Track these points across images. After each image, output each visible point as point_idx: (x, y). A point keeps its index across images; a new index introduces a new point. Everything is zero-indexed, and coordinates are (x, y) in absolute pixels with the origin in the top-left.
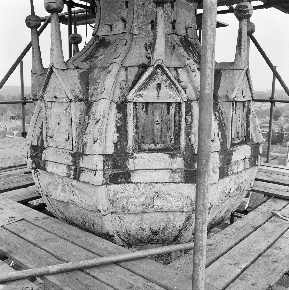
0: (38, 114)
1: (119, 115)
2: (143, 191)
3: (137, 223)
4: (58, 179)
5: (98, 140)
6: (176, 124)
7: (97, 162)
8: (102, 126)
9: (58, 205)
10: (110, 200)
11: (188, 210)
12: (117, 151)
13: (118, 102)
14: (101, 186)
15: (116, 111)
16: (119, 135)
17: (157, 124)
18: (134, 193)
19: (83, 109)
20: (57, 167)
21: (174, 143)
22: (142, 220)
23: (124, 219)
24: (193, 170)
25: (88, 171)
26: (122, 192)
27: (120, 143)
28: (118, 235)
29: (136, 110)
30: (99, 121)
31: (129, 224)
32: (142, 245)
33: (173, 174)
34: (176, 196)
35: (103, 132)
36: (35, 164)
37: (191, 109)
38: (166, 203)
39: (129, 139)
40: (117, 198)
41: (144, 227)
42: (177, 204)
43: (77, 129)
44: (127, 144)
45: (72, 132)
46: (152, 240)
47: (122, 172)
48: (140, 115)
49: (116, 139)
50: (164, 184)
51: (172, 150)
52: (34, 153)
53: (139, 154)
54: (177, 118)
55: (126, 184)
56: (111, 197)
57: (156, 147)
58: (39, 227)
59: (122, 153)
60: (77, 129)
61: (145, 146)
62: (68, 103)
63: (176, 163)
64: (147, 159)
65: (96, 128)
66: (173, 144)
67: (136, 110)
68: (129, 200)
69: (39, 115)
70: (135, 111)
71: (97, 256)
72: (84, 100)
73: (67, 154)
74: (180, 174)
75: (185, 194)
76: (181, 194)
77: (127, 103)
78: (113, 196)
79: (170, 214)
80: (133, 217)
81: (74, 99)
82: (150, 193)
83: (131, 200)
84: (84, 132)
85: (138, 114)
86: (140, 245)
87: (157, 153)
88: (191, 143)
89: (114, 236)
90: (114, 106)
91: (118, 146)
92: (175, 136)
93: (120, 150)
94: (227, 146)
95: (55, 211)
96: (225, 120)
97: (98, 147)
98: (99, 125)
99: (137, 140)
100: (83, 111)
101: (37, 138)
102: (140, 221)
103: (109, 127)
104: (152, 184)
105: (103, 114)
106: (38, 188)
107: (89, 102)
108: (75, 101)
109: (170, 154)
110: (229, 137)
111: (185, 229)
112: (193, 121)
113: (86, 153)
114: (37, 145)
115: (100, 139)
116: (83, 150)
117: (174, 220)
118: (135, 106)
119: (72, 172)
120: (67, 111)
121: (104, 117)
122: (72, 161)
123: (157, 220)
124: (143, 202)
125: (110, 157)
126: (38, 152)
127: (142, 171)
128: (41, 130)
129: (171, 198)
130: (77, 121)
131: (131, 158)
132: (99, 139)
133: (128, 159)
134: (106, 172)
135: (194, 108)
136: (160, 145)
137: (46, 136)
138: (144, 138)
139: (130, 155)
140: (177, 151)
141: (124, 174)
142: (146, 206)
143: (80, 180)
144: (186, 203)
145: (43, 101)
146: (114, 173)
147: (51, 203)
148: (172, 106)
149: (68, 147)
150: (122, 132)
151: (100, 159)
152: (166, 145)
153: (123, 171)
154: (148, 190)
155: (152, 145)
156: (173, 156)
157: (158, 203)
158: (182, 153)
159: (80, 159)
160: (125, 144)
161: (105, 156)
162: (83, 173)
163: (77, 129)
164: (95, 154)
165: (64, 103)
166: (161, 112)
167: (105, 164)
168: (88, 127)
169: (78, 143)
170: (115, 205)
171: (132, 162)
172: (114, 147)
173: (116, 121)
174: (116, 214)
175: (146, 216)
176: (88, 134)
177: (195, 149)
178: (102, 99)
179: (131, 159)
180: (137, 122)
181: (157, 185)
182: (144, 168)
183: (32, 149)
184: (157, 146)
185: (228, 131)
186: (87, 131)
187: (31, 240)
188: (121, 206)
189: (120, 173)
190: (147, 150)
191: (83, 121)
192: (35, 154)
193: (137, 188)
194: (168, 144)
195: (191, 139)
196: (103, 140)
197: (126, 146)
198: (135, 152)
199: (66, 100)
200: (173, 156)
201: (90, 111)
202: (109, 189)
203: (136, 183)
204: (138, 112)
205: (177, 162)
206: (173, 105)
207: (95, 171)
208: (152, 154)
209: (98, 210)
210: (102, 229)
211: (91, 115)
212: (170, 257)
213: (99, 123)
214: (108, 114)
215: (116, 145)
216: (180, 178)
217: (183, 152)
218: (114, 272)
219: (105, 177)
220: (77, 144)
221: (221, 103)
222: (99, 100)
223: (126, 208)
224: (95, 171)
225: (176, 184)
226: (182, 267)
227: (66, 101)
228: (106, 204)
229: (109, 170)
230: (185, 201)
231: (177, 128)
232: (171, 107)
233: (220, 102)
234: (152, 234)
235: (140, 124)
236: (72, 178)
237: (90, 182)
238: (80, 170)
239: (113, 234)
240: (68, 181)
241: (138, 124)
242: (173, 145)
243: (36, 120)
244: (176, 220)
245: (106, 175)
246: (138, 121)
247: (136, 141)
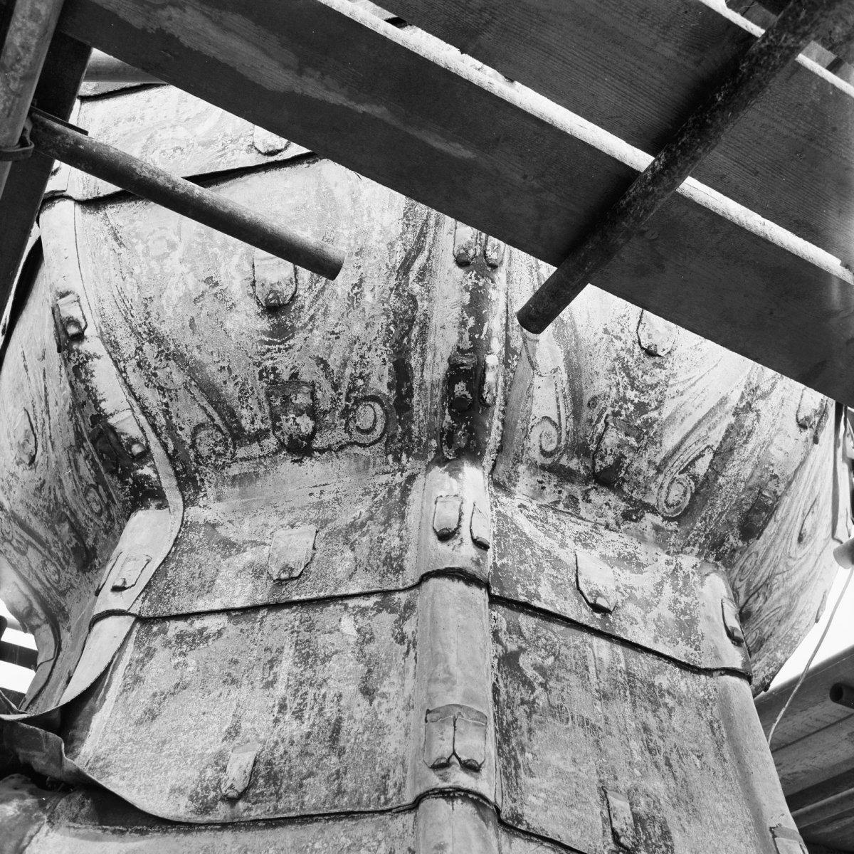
3: (189, 248)
18: (177, 111)
23: (134, 240)
31: (154, 263)
68: (157, 138)
111: (420, 261)
117: (355, 201)
142: (220, 147)
212: (396, 526)
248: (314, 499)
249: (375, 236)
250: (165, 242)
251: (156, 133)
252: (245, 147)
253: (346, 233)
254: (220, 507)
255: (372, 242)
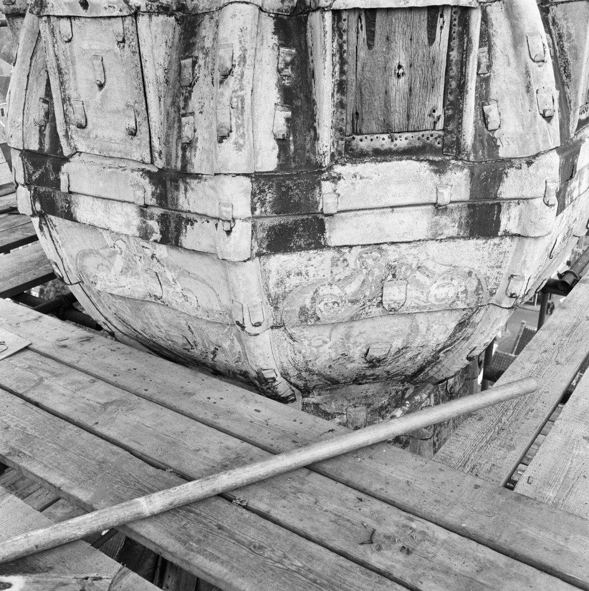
0: (31, 59)
1: (287, 54)
2: (356, 265)
4: (112, 243)
5: (231, 131)
6: (452, 74)
7: (236, 197)
8: (241, 89)
9: (113, 305)
10: (269, 296)
11: (468, 305)
12: (287, 159)
13: (279, 10)
14: (245, 261)
15: (276, 42)
16: (289, 113)
17: (399, 76)
18: (332, 272)
19: (173, 38)
20: (106, 211)
21: (443, 130)
22: (348, 337)
24: (490, 203)
25: (203, 220)
26: (299, 274)
27: (295, 136)
28: (285, 375)
29: (341, 36)
30: (230, 72)
32: (335, 389)
33: (437, 217)
34: (440, 273)
35: (246, 107)
36: (41, 203)
37: (487, 26)
38: (413, 293)
39: (322, 124)
40: (287, 290)
41: (351, 351)
42: (441, 291)
43: (162, 99)
44: (316, 138)
45: (147, 109)
46: (365, 377)
47: (303, 220)
48: (352, 49)
49: (281, 128)
50: (412, 245)
51: (439, 151)
52: (34, 172)
53: (349, 165)
54: (454, 54)
55: (311, 252)
56: (271, 287)
57: (396, 145)
58: (75, 368)
59: (300, 167)
60: (160, 101)
61: (363, 143)
62: (128, 21)
63: (449, 187)
64: (371, 179)
65: (222, 94)
66: (441, 133)
67: (341, 36)
68: (320, 292)
69: (33, 61)
70: (336, 38)
71: (250, 446)
72: (174, 8)
73: (137, 176)
74: (456, 216)
75: (466, 267)
76: (454, 267)
77: (308, 13)
78: (278, 284)
79: (421, 319)
80: (325, 332)
81: (147, 6)
82: (376, 269)
83: (324, 291)
84: (184, 108)
85: (345, 48)
86: (330, 390)
87: (397, 160)
88: (490, 127)
89: (274, 380)
90: (269, 24)
91: (289, 145)
92: (448, 109)
93: (294, 158)
94: (571, 128)
95: (106, 319)
96: (568, 57)
97: (235, 152)
98: (231, 86)
99: (342, 125)
100: (173, 43)
101: (38, 128)
102: (342, 339)
103: (259, 90)
104: (382, 246)
105: (241, 52)
106: (56, 264)
107: (190, 14)
108: (148, 12)
109: (431, 162)
110: (575, 104)
111: (450, 348)
112: (494, 61)
113: (196, 170)
114: (41, 149)
115: (238, 127)
116: (185, 161)
117: (428, 330)
118: (338, 23)
119: (155, 225)
120: (126, 45)
121: (243, 59)
122: (153, 194)
123: (386, 333)
124: (355, 293)
125: (269, 180)
126: (46, 168)
127: (356, 212)
128: (46, 106)
129: (427, 279)
130: (158, 74)
131: (327, 179)
132: (234, 129)
133: (319, 184)
134: (259, 222)
135: (494, 22)
136: (406, 139)
137: (66, 122)
138: (362, 119)
139: (323, 172)
140: (452, 152)
141: (307, 223)
142: (362, 304)
143: (181, 247)
144: (464, 288)
145: (45, 18)
146: (280, 225)
147: (94, 300)
148: (442, 19)
149: (135, 154)
150: (298, 103)
151: (242, 186)
152: (423, 136)
153: (305, 217)
154: (370, 262)
155: (383, 139)
156: (440, 168)
157: (393, 294)
158: (466, 158)
159: (177, 188)
160: (308, 138)
161: (257, 177)
162: (189, 227)
163: (160, 101)
164: (225, 174)
165: (113, 20)
166: (411, 39)
167: (255, 200)
168: (193, 94)
169: (167, 143)
170: (281, 309)
171: (331, 190)
172: (277, 150)
173: (279, 71)
174: (282, 328)
175: (358, 327)
176: (197, 113)
177: (498, 143)
178: (231, 3)
179: (328, 183)
180: (342, 72)
181: (393, 247)
182: (362, 206)
183: (26, 160)
184: (396, 139)
185: (575, 88)
186: (191, 104)
187: (61, 409)
188: (298, 309)
189: (296, 221)
190: (371, 153)
191: (177, 74)
192: (36, 176)
193: (342, 259)
194: (427, 132)
195: (488, 116)
196: (248, 130)
197: (313, 145)
198: (337, 163)
199: (121, 11)
200: (440, 168)
201: (194, 44)
202: (267, 266)
203: (339, 248)
204: (344, 42)
205: (452, 182)
206: (445, 17)
207: (229, 221)
208: (384, 164)
209: (238, 323)
210: (240, 363)
211: (201, 56)
213: (231, 80)
214: (253, 51)
215: (282, 143)
216: (457, 225)
217: (468, 155)
218: (311, 494)
219: (256, 236)
220: (163, 146)
221: (559, 5)
222: (221, 8)
223: (310, 313)
224: (229, 221)
225: (443, 243)
226: (472, 457)
227: (121, 14)
228: (259, 308)
229: (269, 217)
230: (463, 284)
231: (454, 84)
232: (440, 20)
233: (556, 4)
234: (367, 365)
235: (351, 77)
236: (155, 241)
237: (212, 250)
238: (180, 219)
239: (273, 375)
240: (143, 247)
241: (344, 78)
242: (439, 136)
243: (28, 76)
244: (432, 329)
245: (259, 229)
246: (346, 68)
247: (341, 130)
248: (363, 394)
249: (433, 342)
250: (321, 341)
251: (319, 288)
252: (375, 304)
253: (419, 341)
254: (319, 398)
255: (430, 344)
